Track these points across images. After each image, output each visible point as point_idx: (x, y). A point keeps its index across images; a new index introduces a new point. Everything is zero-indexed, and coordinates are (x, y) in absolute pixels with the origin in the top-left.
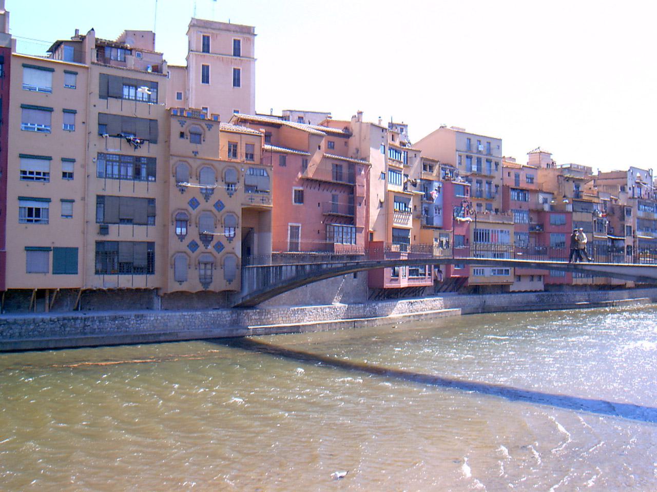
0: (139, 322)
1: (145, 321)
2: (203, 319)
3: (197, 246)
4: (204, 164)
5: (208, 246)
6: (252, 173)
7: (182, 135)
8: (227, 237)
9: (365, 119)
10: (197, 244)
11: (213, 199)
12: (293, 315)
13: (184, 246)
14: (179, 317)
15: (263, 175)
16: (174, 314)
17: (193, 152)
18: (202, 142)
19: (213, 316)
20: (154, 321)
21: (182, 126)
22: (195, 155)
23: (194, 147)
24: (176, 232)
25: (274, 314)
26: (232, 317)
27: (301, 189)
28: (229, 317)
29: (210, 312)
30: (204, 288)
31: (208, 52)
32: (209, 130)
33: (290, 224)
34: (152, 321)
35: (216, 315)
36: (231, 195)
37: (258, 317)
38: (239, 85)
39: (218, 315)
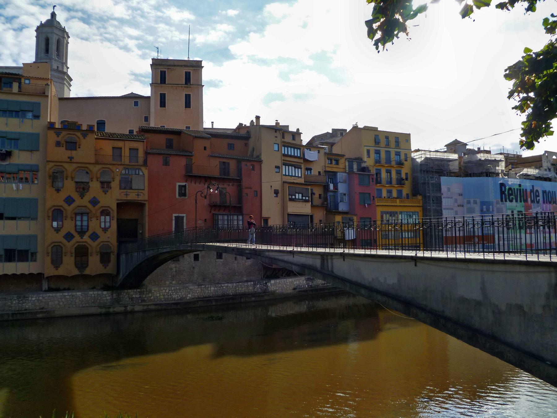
0: (21, 302)
1: (27, 301)
2: (84, 299)
3: (72, 236)
4: (78, 167)
5: (84, 236)
6: (127, 172)
7: (58, 144)
8: (102, 228)
9: (262, 123)
10: (72, 235)
11: (89, 196)
13: (59, 237)
14: (60, 297)
15: (139, 174)
16: (54, 295)
17: (69, 158)
19: (93, 295)
20: (36, 301)
21: (58, 136)
22: (71, 160)
23: (69, 153)
24: (52, 226)
25: (155, 293)
26: (112, 297)
27: (184, 184)
28: (109, 296)
29: (91, 293)
30: (80, 272)
31: (165, 83)
32: (84, 138)
33: (174, 215)
34: (34, 300)
35: (96, 295)
36: (105, 192)
37: (139, 296)
38: (190, 107)
39: (98, 294)
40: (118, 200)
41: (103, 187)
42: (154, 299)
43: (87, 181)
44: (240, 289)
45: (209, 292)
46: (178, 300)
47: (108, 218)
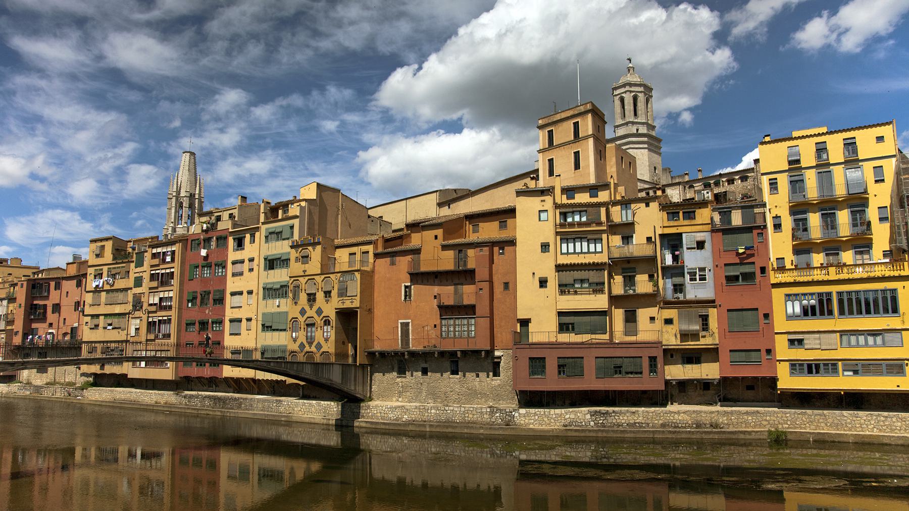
4: (309, 279)
11: (315, 308)
12: (390, 412)
18: (310, 262)
23: (303, 267)
33: (400, 321)
36: (327, 301)
40: (336, 309)
41: (326, 297)
42: (372, 416)
43: (314, 292)
44: (471, 416)
45: (430, 415)
46: (393, 420)
47: (329, 327)
